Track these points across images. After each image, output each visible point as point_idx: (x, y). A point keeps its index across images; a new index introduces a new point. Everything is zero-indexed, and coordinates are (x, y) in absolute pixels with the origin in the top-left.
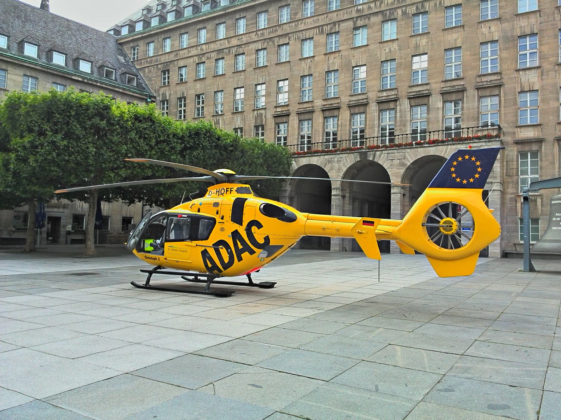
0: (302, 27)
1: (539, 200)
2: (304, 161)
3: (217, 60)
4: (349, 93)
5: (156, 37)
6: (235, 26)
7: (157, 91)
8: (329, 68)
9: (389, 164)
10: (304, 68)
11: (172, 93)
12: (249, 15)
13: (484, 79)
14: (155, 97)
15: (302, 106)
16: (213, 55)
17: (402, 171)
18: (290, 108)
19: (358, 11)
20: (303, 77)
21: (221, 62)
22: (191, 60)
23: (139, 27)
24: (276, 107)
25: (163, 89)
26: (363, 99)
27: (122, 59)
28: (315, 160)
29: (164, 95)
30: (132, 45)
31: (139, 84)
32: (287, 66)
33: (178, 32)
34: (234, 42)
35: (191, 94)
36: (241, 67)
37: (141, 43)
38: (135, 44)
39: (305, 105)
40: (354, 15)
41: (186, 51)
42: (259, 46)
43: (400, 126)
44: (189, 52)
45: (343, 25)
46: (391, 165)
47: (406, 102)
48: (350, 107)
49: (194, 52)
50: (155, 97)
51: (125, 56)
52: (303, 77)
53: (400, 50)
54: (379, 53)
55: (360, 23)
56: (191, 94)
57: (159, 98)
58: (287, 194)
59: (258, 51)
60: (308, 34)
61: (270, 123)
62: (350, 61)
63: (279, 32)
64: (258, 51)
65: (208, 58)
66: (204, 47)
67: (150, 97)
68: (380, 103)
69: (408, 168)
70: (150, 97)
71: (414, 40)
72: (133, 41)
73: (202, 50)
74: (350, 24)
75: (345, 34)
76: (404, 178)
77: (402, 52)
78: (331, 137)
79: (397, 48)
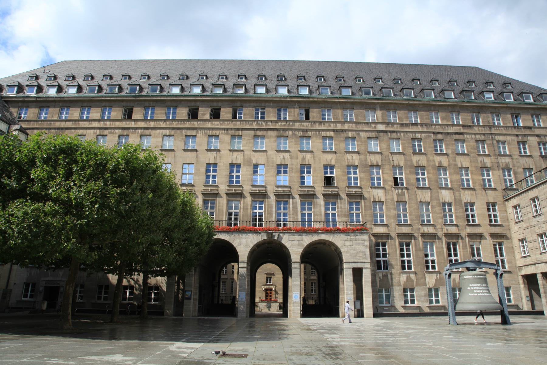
1: (389, 276)
4: (250, 183)
8: (232, 161)
9: (290, 244)
17: (301, 250)
18: (196, 189)
26: (263, 190)
43: (293, 214)
46: (292, 245)
54: (275, 158)
55: (259, 133)
75: (247, 138)
77: (293, 160)
78: (233, 217)
79: (289, 157)
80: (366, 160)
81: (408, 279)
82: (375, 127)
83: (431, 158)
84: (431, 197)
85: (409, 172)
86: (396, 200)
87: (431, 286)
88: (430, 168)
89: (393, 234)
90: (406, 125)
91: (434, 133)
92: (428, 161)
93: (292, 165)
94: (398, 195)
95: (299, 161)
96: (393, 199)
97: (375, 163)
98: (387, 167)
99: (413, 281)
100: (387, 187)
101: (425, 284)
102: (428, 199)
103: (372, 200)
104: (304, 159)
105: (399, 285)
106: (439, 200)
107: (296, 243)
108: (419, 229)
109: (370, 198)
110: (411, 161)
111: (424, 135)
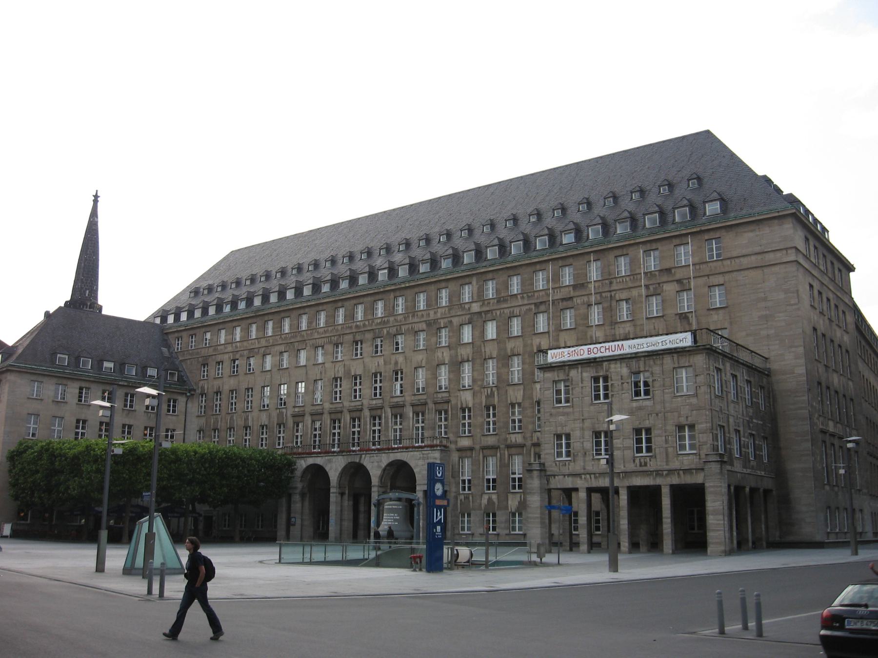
0: (316, 336)
2: (311, 461)
3: (248, 358)
5: (198, 330)
6: (264, 328)
7: (197, 384)
10: (314, 373)
11: (209, 386)
12: (277, 317)
13: (440, 395)
14: (195, 390)
15: (314, 408)
16: (246, 353)
19: (357, 326)
20: (315, 381)
21: (252, 361)
22: (226, 356)
23: (184, 317)
24: (294, 407)
25: (202, 382)
27: (165, 350)
28: (319, 461)
29: (203, 388)
30: (176, 335)
31: (180, 378)
32: (303, 371)
33: (217, 328)
34: (263, 342)
35: (226, 389)
36: (268, 367)
37: (184, 334)
38: (180, 334)
39: (317, 407)
40: (354, 330)
41: (222, 347)
42: (282, 348)
44: (226, 348)
45: (346, 337)
47: (389, 410)
48: (350, 411)
49: (230, 349)
50: (195, 390)
51: (168, 346)
52: (315, 381)
53: (385, 364)
56: (226, 389)
57: (199, 391)
58: (298, 491)
59: (281, 353)
60: (320, 342)
61: (290, 422)
62: (350, 370)
63: (299, 339)
64: (281, 353)
65: (241, 356)
66: (238, 344)
67: (190, 391)
68: (371, 409)
69: (384, 470)
70: (190, 391)
71: (393, 358)
72: (177, 331)
73: (236, 347)
74: (349, 338)
76: (381, 477)
80: (457, 355)
81: (490, 500)
82: (469, 309)
83: (529, 342)
84: (524, 396)
85: (500, 365)
86: (484, 404)
87: (513, 510)
88: (526, 356)
89: (477, 447)
90: (505, 301)
91: (535, 304)
92: (525, 346)
93: (385, 372)
94: (487, 397)
95: (392, 367)
96: (481, 403)
97: (466, 358)
98: (478, 361)
99: (494, 503)
100: (477, 388)
101: (507, 508)
102: (520, 400)
103: (459, 406)
104: (396, 363)
105: (480, 509)
106: (532, 398)
107: (376, 464)
108: (506, 440)
109: (457, 404)
110: (506, 349)
111: (524, 308)
